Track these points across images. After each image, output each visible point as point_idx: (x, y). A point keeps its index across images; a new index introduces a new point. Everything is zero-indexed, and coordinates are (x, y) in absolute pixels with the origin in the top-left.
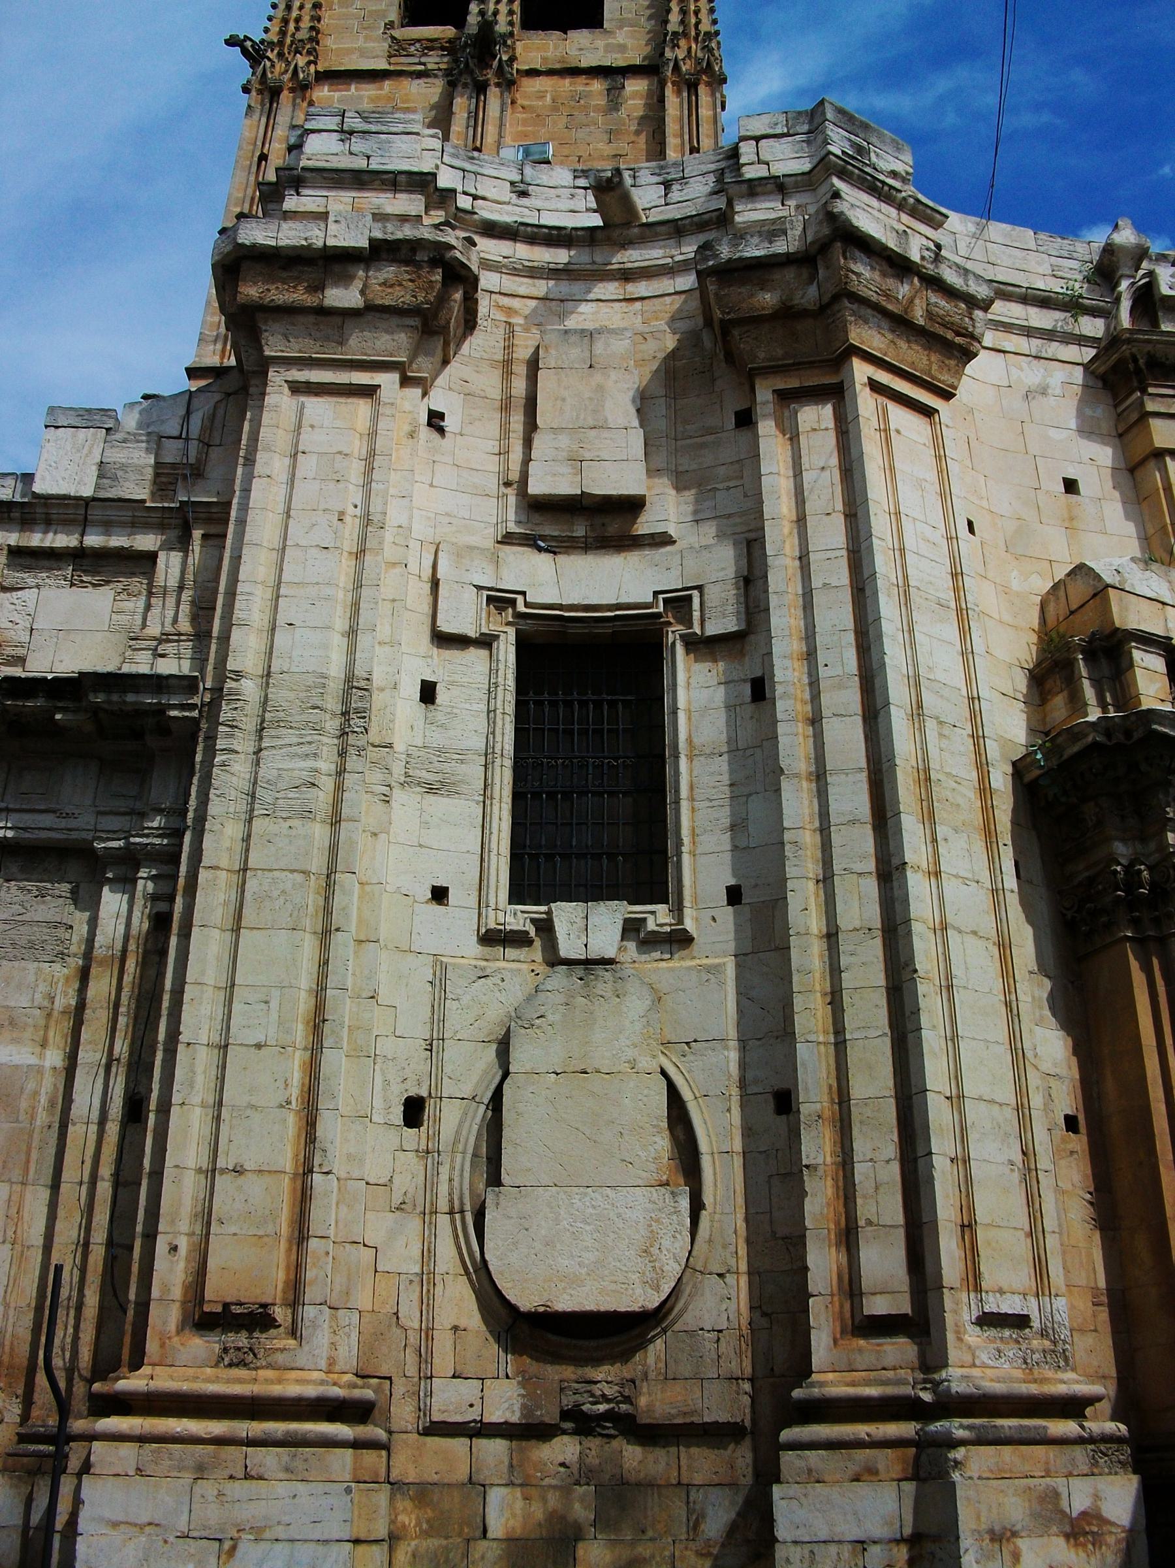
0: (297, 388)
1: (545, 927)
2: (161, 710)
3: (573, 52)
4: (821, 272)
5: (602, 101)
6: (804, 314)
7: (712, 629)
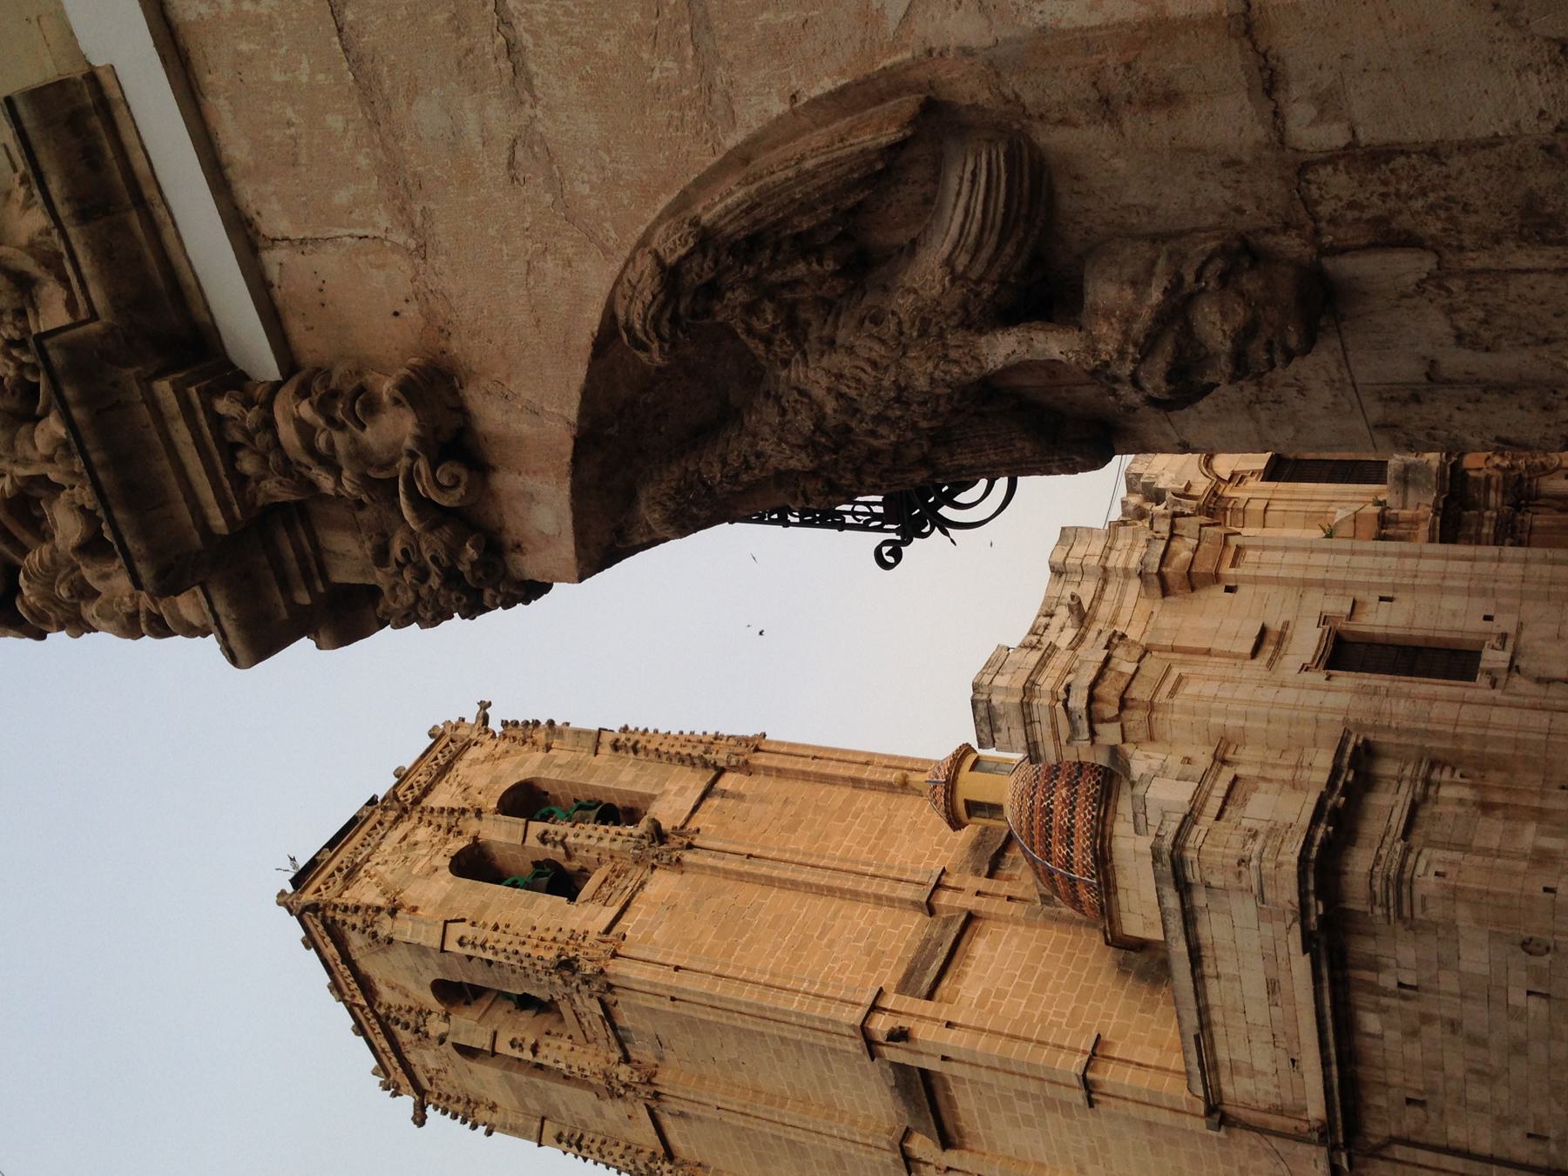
0: (1173, 693)
1: (1489, 672)
2: (1356, 748)
3: (671, 812)
4: (1184, 533)
5: (731, 803)
6: (1198, 545)
7: (1348, 609)
